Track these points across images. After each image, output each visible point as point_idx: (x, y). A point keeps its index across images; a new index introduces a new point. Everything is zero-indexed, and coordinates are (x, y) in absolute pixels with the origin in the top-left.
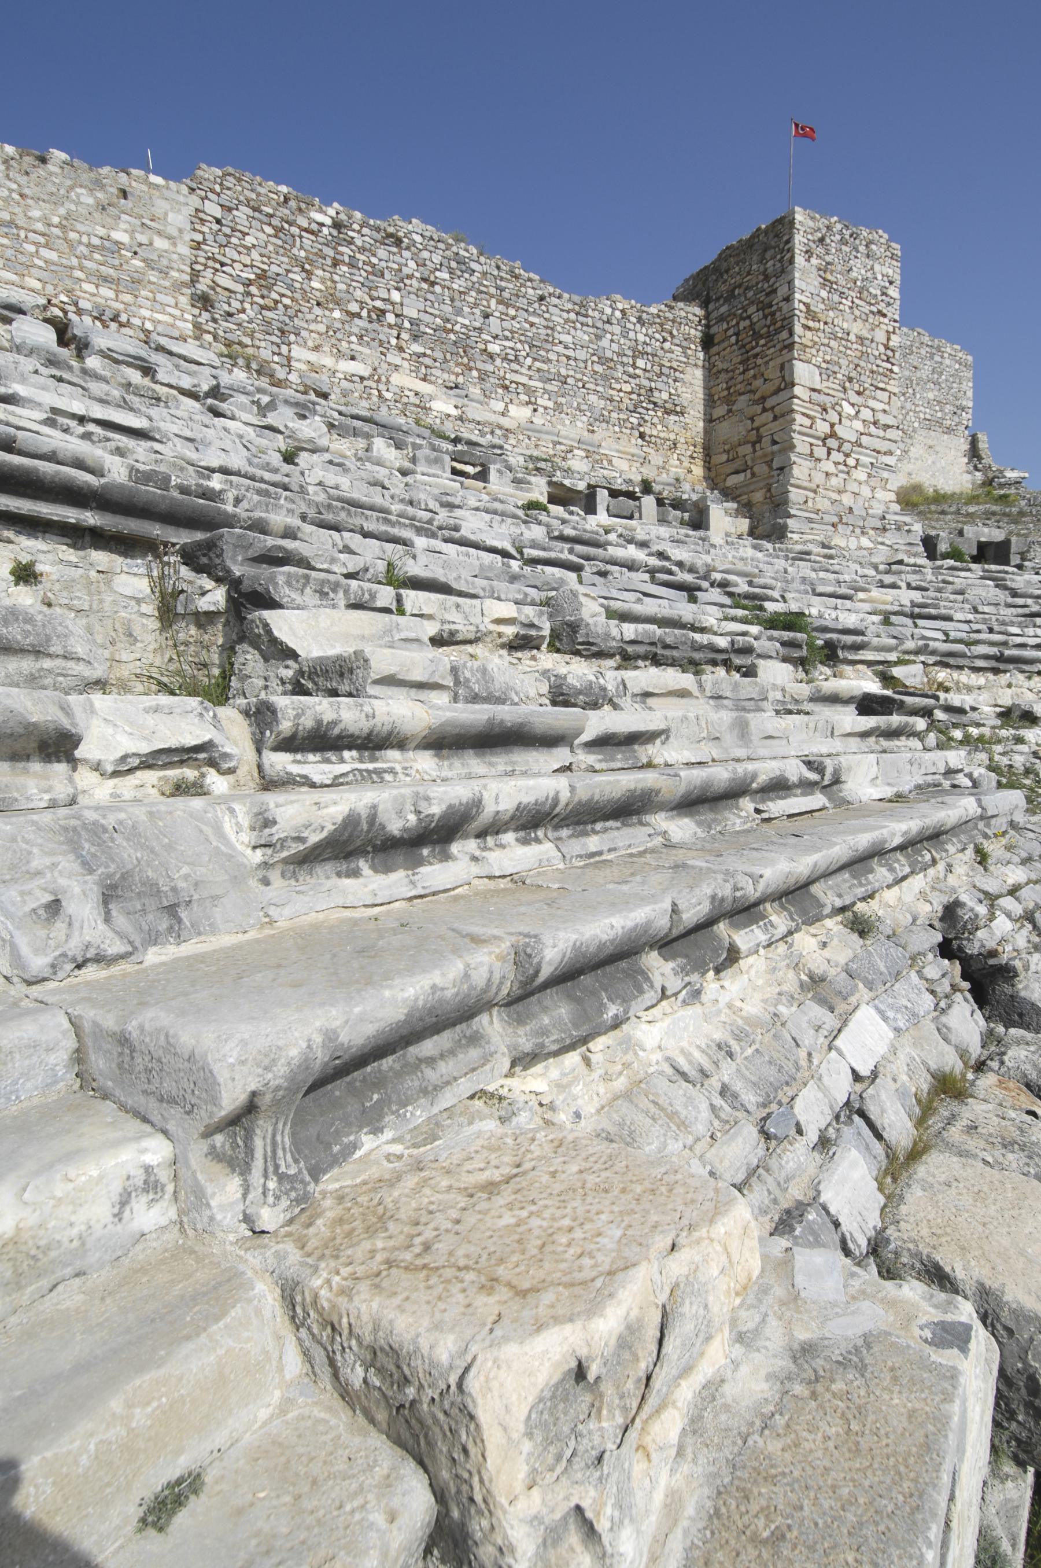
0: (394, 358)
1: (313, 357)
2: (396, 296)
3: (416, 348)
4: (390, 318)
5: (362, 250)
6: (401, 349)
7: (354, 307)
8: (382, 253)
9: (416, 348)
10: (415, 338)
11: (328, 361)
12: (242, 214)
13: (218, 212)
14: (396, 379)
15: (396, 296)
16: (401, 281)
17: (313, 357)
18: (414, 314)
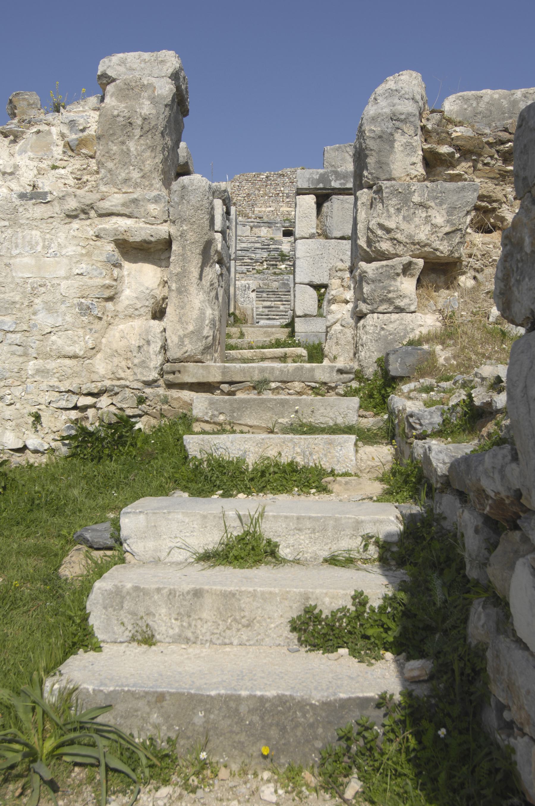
0: (281, 204)
1: (260, 209)
2: (282, 189)
3: (288, 200)
4: (281, 195)
5: (273, 181)
6: (283, 201)
7: (271, 195)
8: (279, 180)
9: (288, 200)
10: (287, 197)
11: (264, 209)
12: (243, 183)
13: (238, 184)
14: (281, 209)
15: (282, 189)
16: (284, 185)
17: (260, 209)
18: (287, 192)
